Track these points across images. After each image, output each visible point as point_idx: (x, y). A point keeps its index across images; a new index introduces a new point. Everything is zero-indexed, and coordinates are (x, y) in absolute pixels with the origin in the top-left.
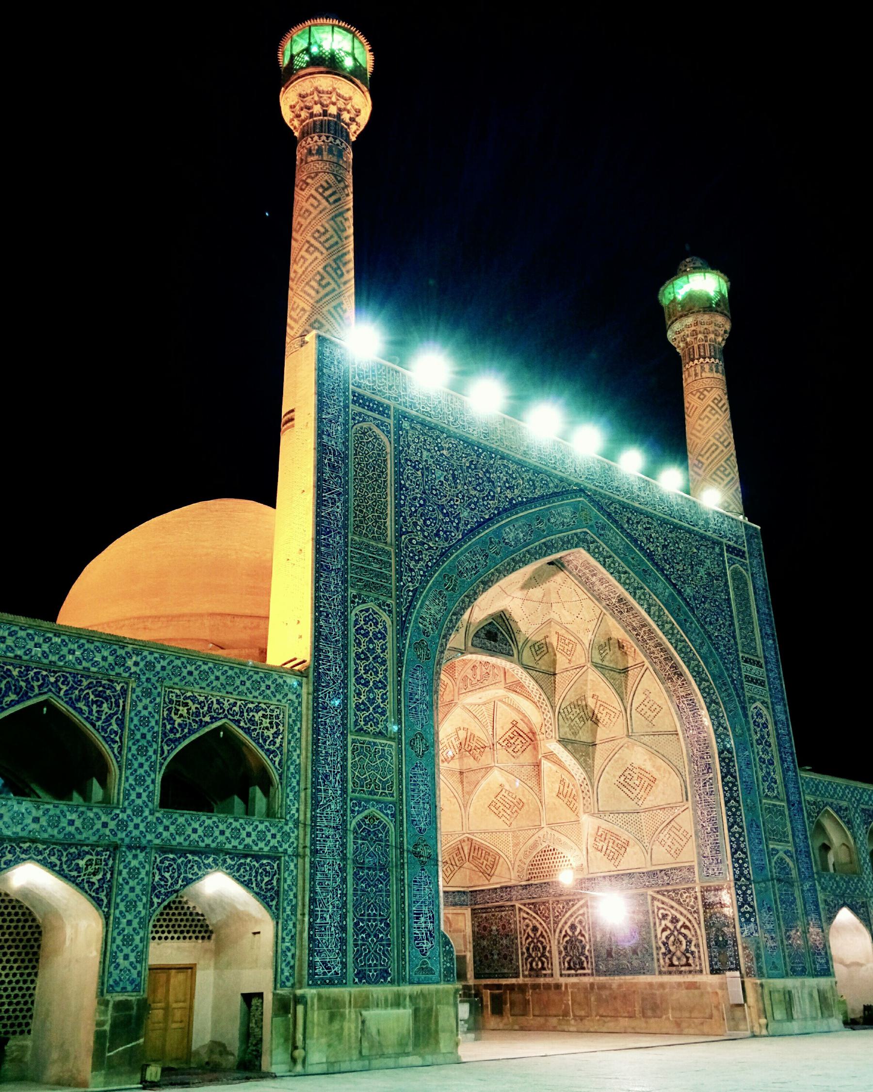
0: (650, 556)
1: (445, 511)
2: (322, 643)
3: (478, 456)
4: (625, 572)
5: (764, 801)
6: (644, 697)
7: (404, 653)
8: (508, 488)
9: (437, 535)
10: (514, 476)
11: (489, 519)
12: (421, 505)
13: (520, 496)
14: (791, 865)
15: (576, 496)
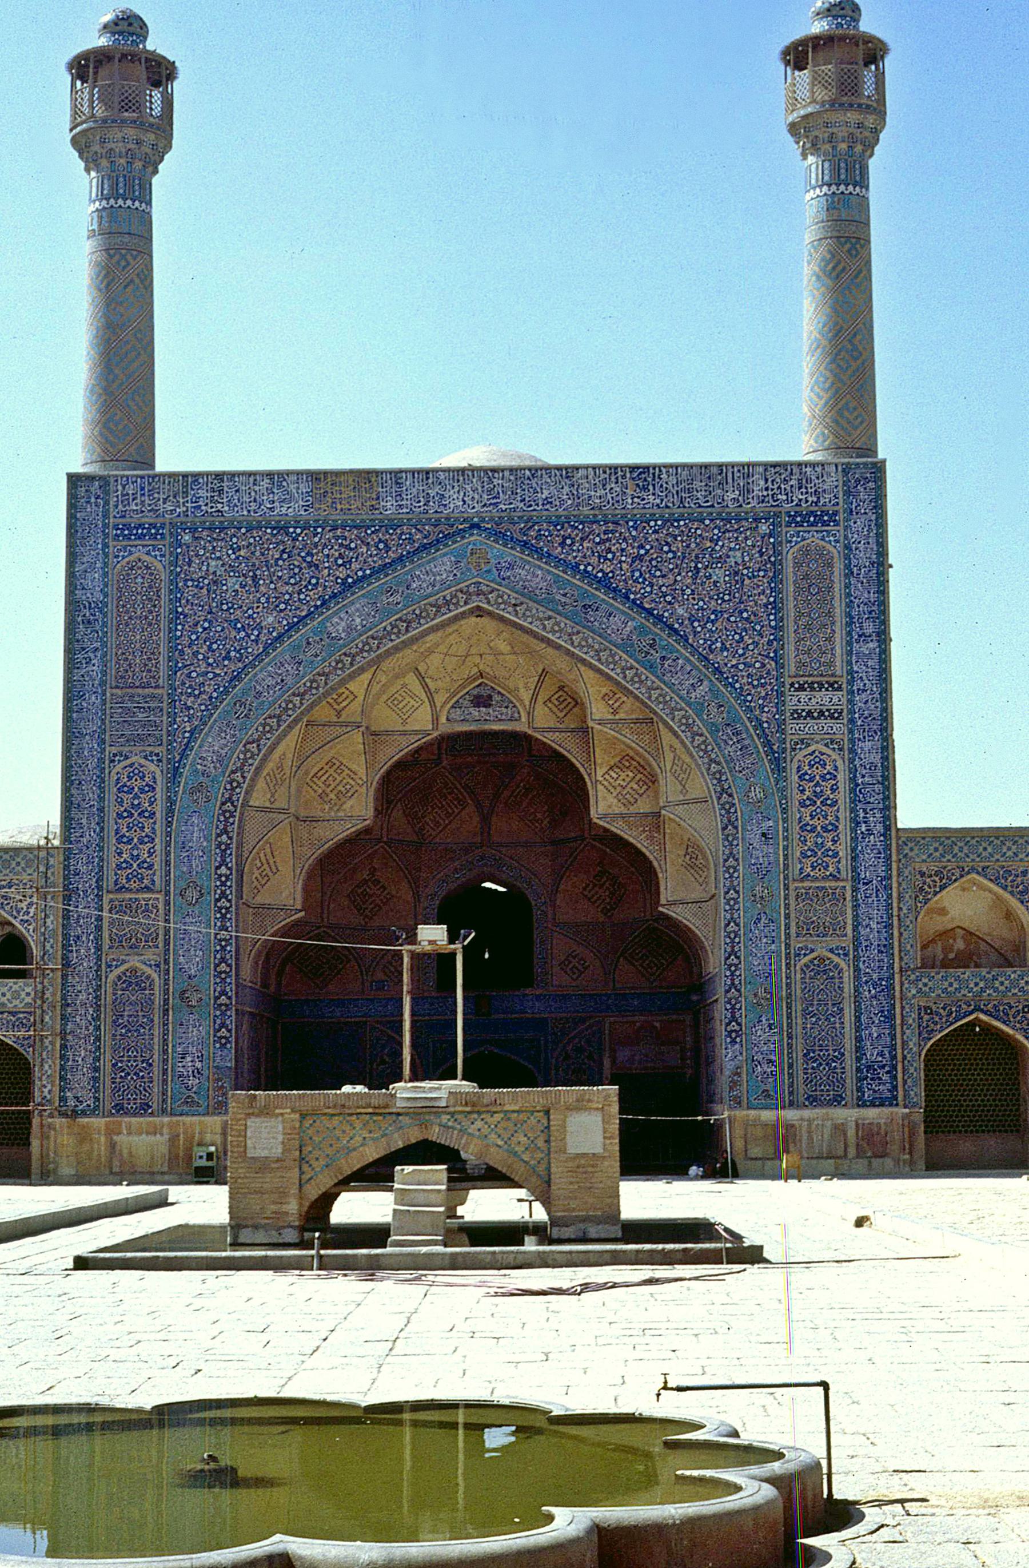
0: (605, 582)
1: (239, 625)
2: (74, 811)
3: (295, 539)
4: (550, 618)
5: (792, 887)
6: (672, 755)
7: (175, 801)
8: (340, 566)
9: (227, 657)
10: (353, 545)
11: (306, 616)
12: (205, 629)
13: (361, 569)
14: (843, 965)
15: (463, 538)
